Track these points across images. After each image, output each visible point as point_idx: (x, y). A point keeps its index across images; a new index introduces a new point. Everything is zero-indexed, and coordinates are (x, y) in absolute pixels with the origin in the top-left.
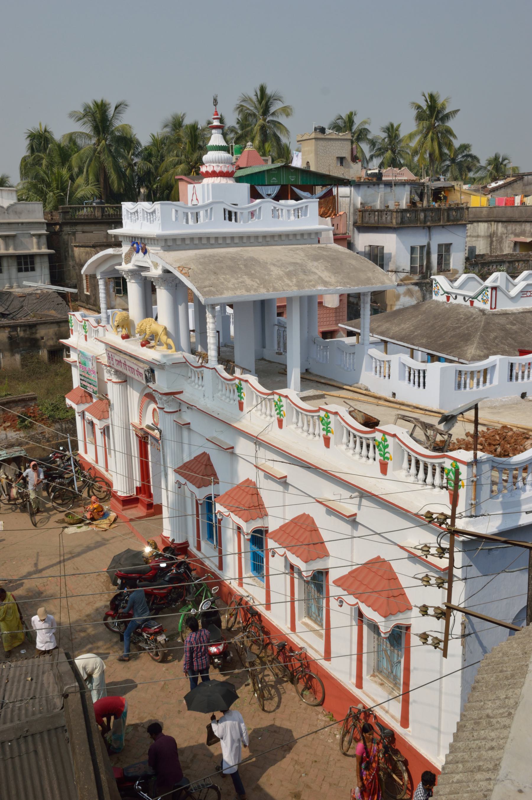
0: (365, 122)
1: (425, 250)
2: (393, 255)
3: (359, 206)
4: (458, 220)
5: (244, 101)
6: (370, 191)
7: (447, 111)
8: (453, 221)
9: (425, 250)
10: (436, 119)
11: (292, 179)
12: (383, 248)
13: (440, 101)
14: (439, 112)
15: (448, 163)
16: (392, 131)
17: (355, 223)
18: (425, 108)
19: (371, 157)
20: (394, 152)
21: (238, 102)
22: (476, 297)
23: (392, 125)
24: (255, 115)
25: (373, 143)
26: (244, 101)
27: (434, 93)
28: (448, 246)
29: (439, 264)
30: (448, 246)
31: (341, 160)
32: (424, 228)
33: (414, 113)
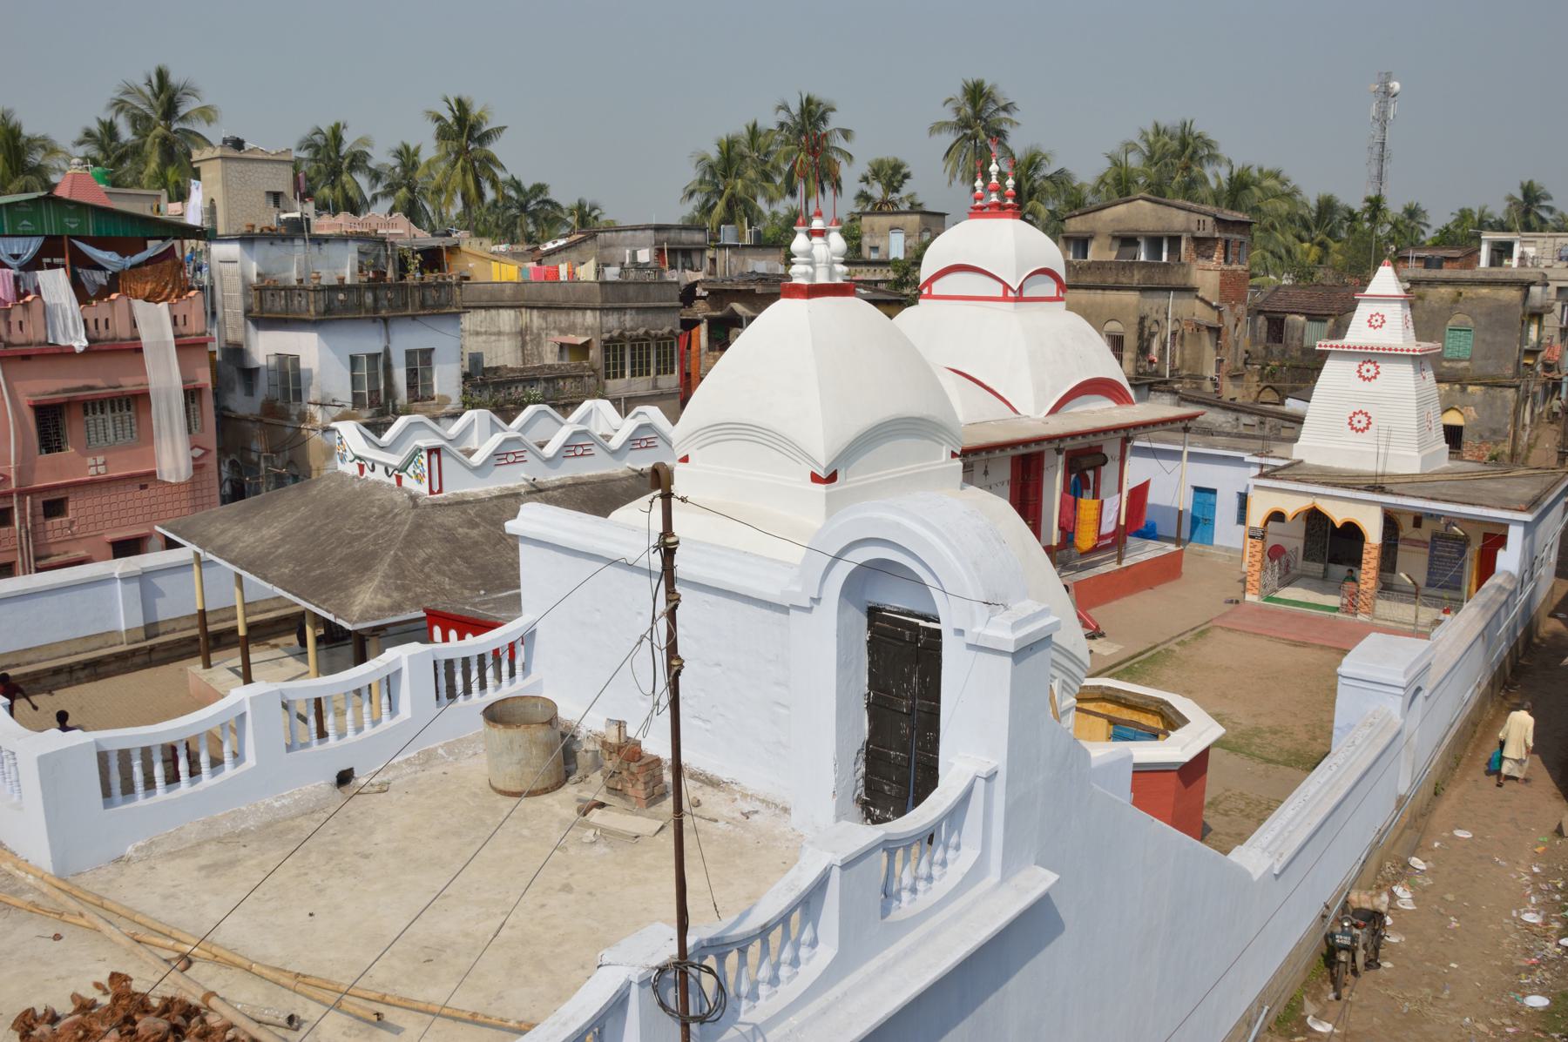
1: (381, 360)
2: (315, 371)
3: (254, 279)
4: (442, 306)
5: (127, 93)
6: (276, 252)
7: (485, 128)
8: (433, 307)
9: (381, 360)
10: (469, 138)
12: (296, 359)
13: (475, 110)
14: (473, 128)
15: (514, 211)
16: (407, 157)
17: (248, 313)
18: (451, 120)
19: (375, 198)
20: (411, 189)
21: (116, 95)
22: (404, 469)
23: (407, 148)
24: (148, 118)
25: (376, 176)
26: (127, 93)
27: (464, 98)
28: (427, 354)
29: (411, 386)
30: (427, 354)
31: (276, 197)
32: (374, 320)
33: (433, 128)
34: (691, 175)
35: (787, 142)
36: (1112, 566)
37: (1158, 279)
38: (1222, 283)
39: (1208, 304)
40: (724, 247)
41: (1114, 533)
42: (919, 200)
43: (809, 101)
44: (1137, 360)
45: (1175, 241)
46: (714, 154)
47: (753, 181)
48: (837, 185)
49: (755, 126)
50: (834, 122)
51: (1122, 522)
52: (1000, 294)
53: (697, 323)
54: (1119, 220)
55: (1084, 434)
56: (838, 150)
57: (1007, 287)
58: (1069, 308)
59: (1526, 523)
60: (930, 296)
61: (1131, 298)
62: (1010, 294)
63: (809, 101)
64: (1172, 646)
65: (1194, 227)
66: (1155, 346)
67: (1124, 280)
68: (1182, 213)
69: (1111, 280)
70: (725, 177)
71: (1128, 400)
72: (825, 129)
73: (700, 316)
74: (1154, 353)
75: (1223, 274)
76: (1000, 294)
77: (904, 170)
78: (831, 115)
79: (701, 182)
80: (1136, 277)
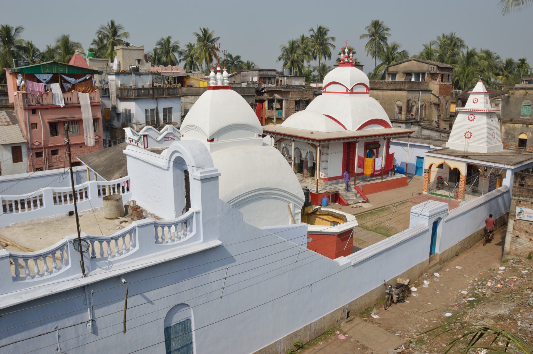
0: (176, 42)
1: (155, 111)
2: (135, 114)
3: (119, 86)
4: (175, 95)
5: (102, 28)
6: (126, 78)
7: (213, 38)
8: (172, 95)
9: (155, 111)
10: (208, 41)
11: (61, 70)
12: (130, 110)
13: (210, 32)
14: (208, 38)
15: (230, 65)
16: (190, 47)
17: (117, 96)
18: (202, 36)
19: (180, 61)
20: (192, 58)
21: (99, 29)
22: (138, 141)
23: (191, 44)
24: (108, 36)
25: (181, 53)
26: (102, 28)
27: (206, 28)
28: (170, 109)
29: (165, 119)
30: (170, 109)
31: (139, 61)
32: (153, 99)
33: (196, 38)
34: (280, 53)
35: (312, 42)
36: (380, 181)
37: (415, 87)
38: (440, 89)
39: (435, 96)
40: (285, 76)
41: (381, 170)
42: (358, 61)
43: (320, 28)
44: (406, 114)
45: (424, 74)
46: (288, 46)
47: (300, 55)
48: (330, 56)
49: (303, 36)
50: (329, 35)
51: (383, 166)
52: (345, 91)
53: (264, 101)
54: (406, 67)
55: (371, 136)
56: (330, 44)
57: (347, 89)
58: (370, 96)
59: (512, 169)
60: (325, 92)
61: (404, 93)
62: (349, 91)
63: (320, 28)
64: (390, 206)
65: (430, 70)
66: (414, 110)
67: (402, 87)
68: (426, 65)
69: (398, 88)
70: (291, 53)
71: (390, 127)
72: (326, 37)
73: (265, 99)
74: (414, 112)
75: (441, 85)
76: (345, 91)
77: (354, 51)
78: (328, 32)
79: (283, 55)
80: (406, 87)
